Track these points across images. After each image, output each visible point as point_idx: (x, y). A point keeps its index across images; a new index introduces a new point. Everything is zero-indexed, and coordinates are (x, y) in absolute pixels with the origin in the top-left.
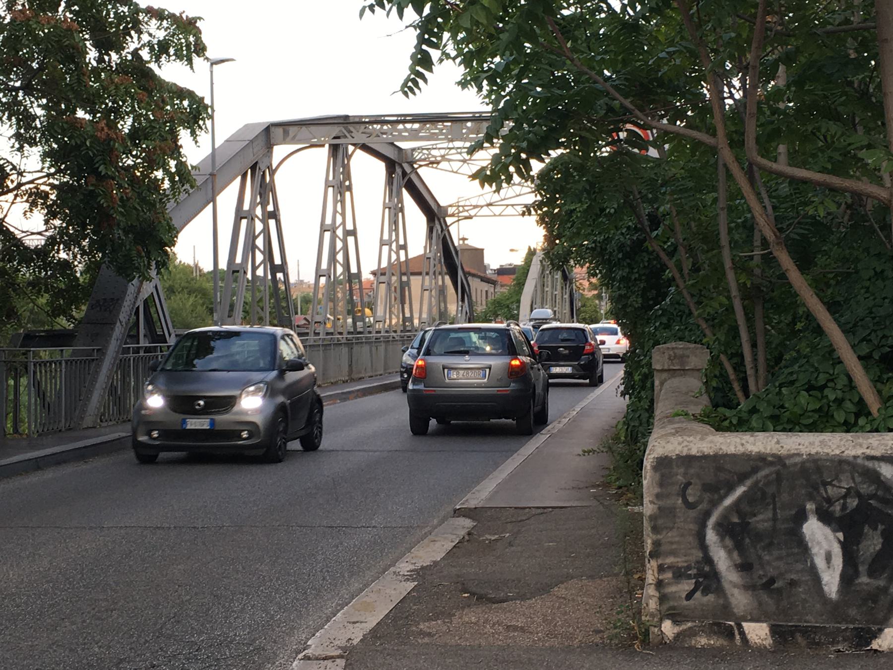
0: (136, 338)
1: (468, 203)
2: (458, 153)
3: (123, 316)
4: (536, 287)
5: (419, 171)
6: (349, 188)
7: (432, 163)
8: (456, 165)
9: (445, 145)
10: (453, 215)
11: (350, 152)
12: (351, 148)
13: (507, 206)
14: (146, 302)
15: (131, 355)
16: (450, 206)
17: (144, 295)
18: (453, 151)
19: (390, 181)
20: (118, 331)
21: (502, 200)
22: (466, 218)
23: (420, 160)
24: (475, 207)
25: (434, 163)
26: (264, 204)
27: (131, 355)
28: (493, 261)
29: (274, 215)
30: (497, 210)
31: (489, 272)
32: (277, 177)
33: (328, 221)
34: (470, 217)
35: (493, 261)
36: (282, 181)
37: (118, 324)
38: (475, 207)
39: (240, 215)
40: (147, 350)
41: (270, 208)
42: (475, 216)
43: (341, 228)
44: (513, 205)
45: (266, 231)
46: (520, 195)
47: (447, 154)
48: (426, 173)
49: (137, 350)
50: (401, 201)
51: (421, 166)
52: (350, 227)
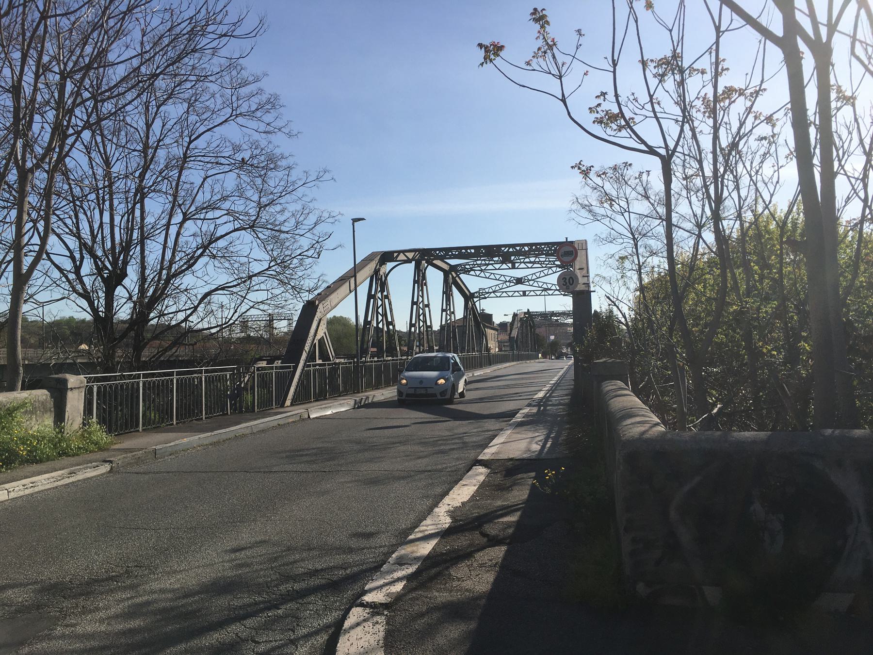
0: (314, 359)
1: (484, 291)
3: (307, 348)
6: (425, 284)
7: (466, 272)
8: (478, 273)
9: (472, 263)
10: (477, 297)
13: (503, 292)
14: (319, 341)
15: (312, 368)
17: (318, 337)
20: (304, 356)
21: (500, 289)
22: (483, 298)
23: (461, 270)
24: (488, 293)
25: (467, 272)
26: (382, 291)
27: (312, 368)
28: (497, 320)
29: (387, 297)
30: (498, 294)
31: (495, 325)
33: (415, 300)
34: (485, 298)
35: (497, 320)
36: (392, 281)
37: (304, 351)
38: (488, 293)
39: (370, 296)
40: (320, 365)
41: (385, 293)
42: (488, 297)
44: (506, 292)
45: (383, 305)
46: (509, 287)
47: (474, 267)
49: (315, 366)
50: (451, 290)
51: (461, 273)
52: (426, 302)
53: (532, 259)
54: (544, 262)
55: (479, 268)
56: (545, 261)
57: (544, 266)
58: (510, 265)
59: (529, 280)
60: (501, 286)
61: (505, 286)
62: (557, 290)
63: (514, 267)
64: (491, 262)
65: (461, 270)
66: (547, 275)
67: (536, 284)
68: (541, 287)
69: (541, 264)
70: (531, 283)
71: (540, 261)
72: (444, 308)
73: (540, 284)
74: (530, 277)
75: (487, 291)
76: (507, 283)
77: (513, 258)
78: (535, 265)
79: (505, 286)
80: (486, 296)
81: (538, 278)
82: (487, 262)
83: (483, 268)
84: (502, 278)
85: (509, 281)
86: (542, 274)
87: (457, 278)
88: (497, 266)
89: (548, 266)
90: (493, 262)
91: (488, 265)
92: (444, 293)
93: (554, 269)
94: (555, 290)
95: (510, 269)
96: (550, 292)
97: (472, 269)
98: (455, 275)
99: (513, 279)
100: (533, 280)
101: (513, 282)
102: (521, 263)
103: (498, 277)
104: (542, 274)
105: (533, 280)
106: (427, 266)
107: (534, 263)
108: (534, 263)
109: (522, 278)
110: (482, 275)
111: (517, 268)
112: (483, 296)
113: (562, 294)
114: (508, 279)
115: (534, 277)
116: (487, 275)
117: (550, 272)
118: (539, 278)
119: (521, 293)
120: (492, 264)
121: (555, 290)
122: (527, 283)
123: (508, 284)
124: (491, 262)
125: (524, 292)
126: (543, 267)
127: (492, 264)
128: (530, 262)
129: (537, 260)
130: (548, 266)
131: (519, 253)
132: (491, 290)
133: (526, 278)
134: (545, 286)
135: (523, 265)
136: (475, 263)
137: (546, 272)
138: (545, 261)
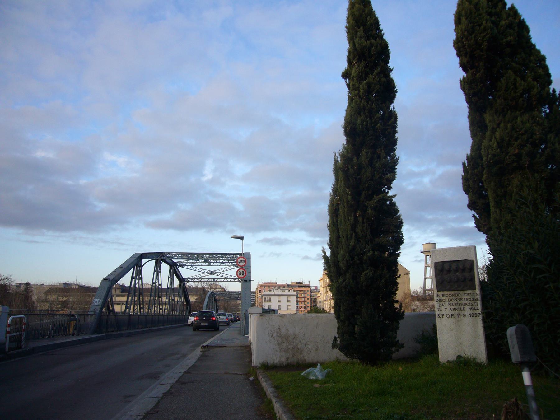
1: (192, 278)
2: (190, 264)
4: (207, 302)
5: (178, 268)
6: (160, 272)
7: (183, 266)
8: (189, 267)
9: (187, 261)
10: (187, 281)
11: (161, 262)
12: (161, 261)
16: (187, 278)
18: (189, 263)
19: (170, 271)
25: (182, 266)
32: (143, 268)
36: (144, 269)
38: (194, 279)
42: (193, 281)
43: (157, 283)
47: (187, 264)
48: (180, 269)
50: (173, 276)
51: (179, 267)
52: (160, 283)
53: (221, 261)
54: (227, 263)
55: (190, 265)
56: (228, 262)
57: (227, 265)
58: (208, 263)
59: (217, 273)
60: (202, 275)
61: (204, 275)
62: (232, 279)
63: (210, 265)
64: (197, 261)
65: (179, 265)
66: (228, 270)
67: (221, 275)
68: (224, 277)
69: (225, 264)
70: (219, 274)
71: (225, 262)
72: (154, 281)
73: (224, 275)
74: (218, 271)
75: (193, 277)
76: (205, 274)
77: (210, 260)
78: (222, 264)
79: (204, 275)
80: (192, 280)
81: (223, 272)
82: (195, 261)
83: (192, 264)
84: (203, 271)
85: (206, 273)
86: (225, 270)
87: (177, 270)
88: (200, 264)
89: (229, 265)
90: (199, 262)
91: (196, 263)
92: (169, 278)
93: (232, 267)
94: (232, 279)
95: (207, 266)
96: (229, 280)
97: (186, 265)
98: (176, 268)
99: (208, 271)
100: (220, 273)
101: (209, 274)
102: (214, 263)
103: (200, 270)
104: (225, 270)
105: (220, 273)
106: (162, 263)
107: (221, 263)
108: (221, 263)
109: (213, 271)
110: (191, 268)
111: (211, 266)
112: (190, 281)
113: (235, 281)
114: (206, 271)
115: (221, 271)
116: (195, 269)
117: (230, 268)
118: (223, 271)
119: (213, 280)
120: (198, 263)
121: (232, 279)
122: (216, 274)
123: (206, 274)
124: (197, 261)
125: (214, 279)
126: (226, 266)
127: (198, 263)
128: (220, 263)
129: (224, 261)
130: (229, 265)
131: (213, 258)
132: (196, 277)
133: (216, 271)
134: (226, 276)
135: (215, 264)
136: (188, 261)
137: (227, 268)
138: (228, 262)
